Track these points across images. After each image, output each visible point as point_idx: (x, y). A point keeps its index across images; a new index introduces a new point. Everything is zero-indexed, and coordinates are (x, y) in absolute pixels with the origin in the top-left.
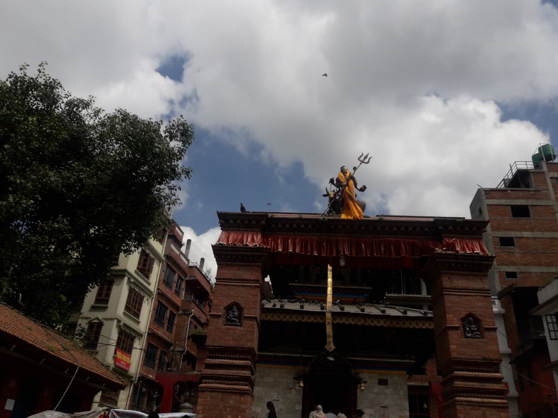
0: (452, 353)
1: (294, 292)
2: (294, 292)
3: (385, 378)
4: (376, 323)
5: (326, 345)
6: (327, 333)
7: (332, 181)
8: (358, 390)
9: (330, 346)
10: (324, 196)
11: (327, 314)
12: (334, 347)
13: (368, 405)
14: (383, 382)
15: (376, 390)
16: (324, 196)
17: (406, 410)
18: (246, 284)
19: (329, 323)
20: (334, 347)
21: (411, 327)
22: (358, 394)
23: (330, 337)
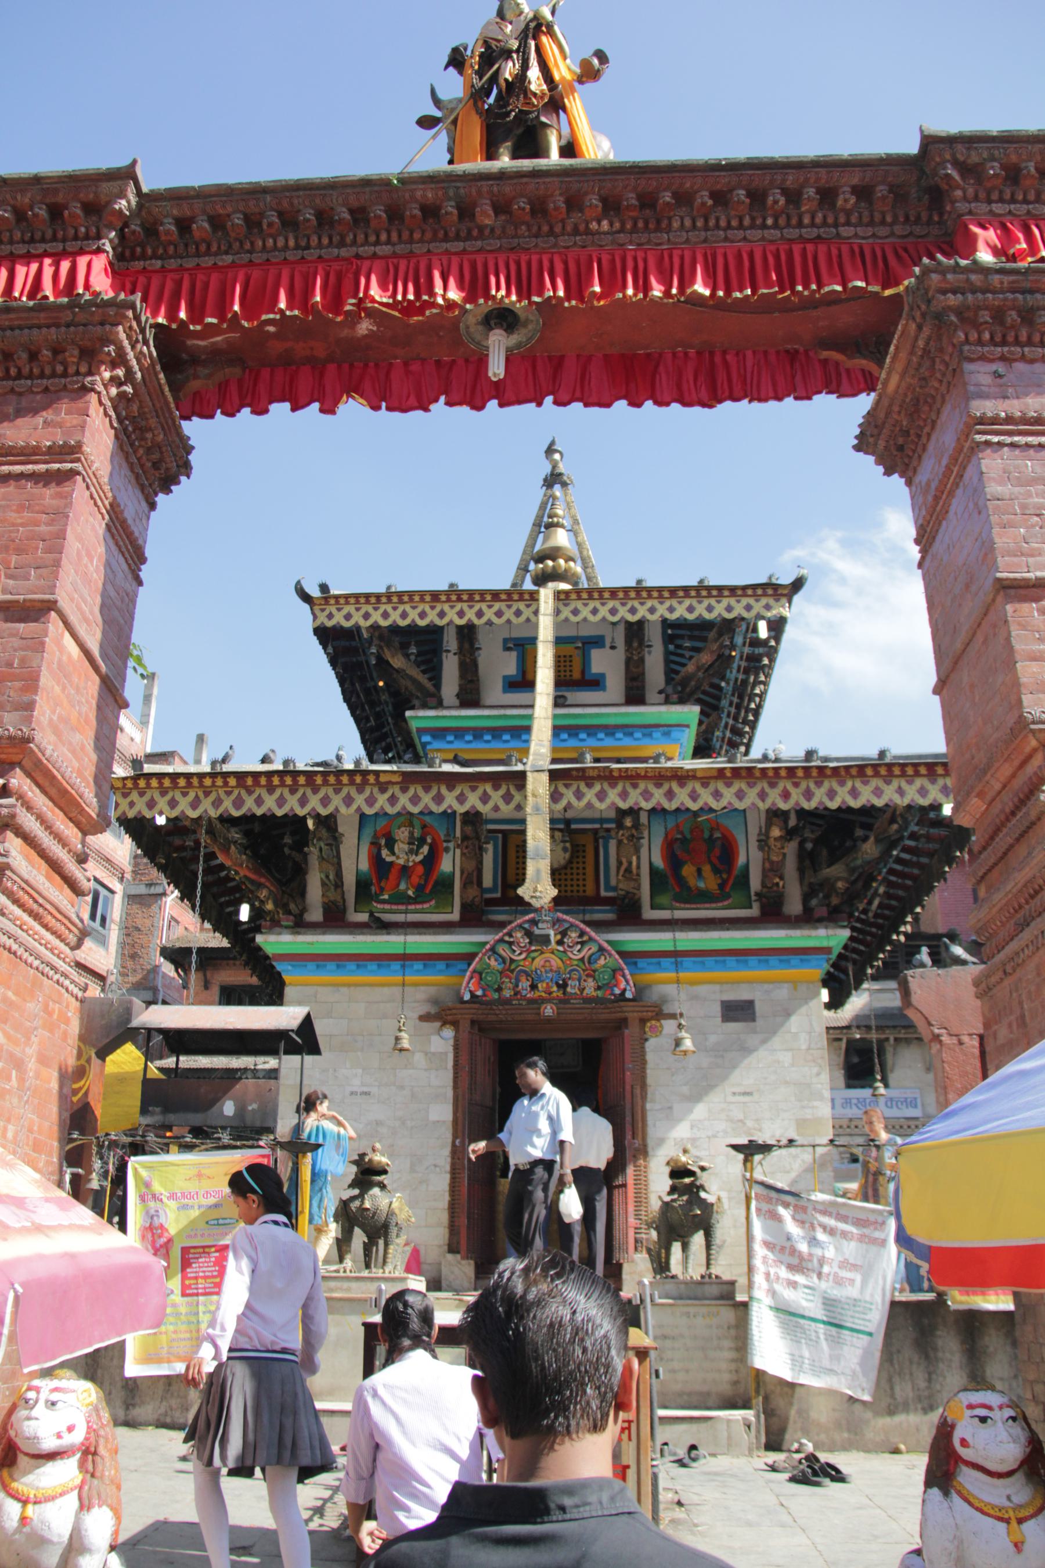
0: (1027, 699)
1: (426, 738)
2: (426, 738)
3: (743, 994)
4: (706, 797)
5: (521, 880)
6: (531, 844)
7: (456, 60)
8: (651, 1045)
9: (539, 886)
10: (426, 122)
11: (530, 777)
12: (554, 892)
13: (685, 1090)
14: (738, 1011)
15: (713, 1039)
16: (426, 122)
17: (821, 1098)
18: (18, 469)
19: (537, 809)
20: (554, 892)
21: (833, 805)
22: (650, 1057)
23: (538, 856)
